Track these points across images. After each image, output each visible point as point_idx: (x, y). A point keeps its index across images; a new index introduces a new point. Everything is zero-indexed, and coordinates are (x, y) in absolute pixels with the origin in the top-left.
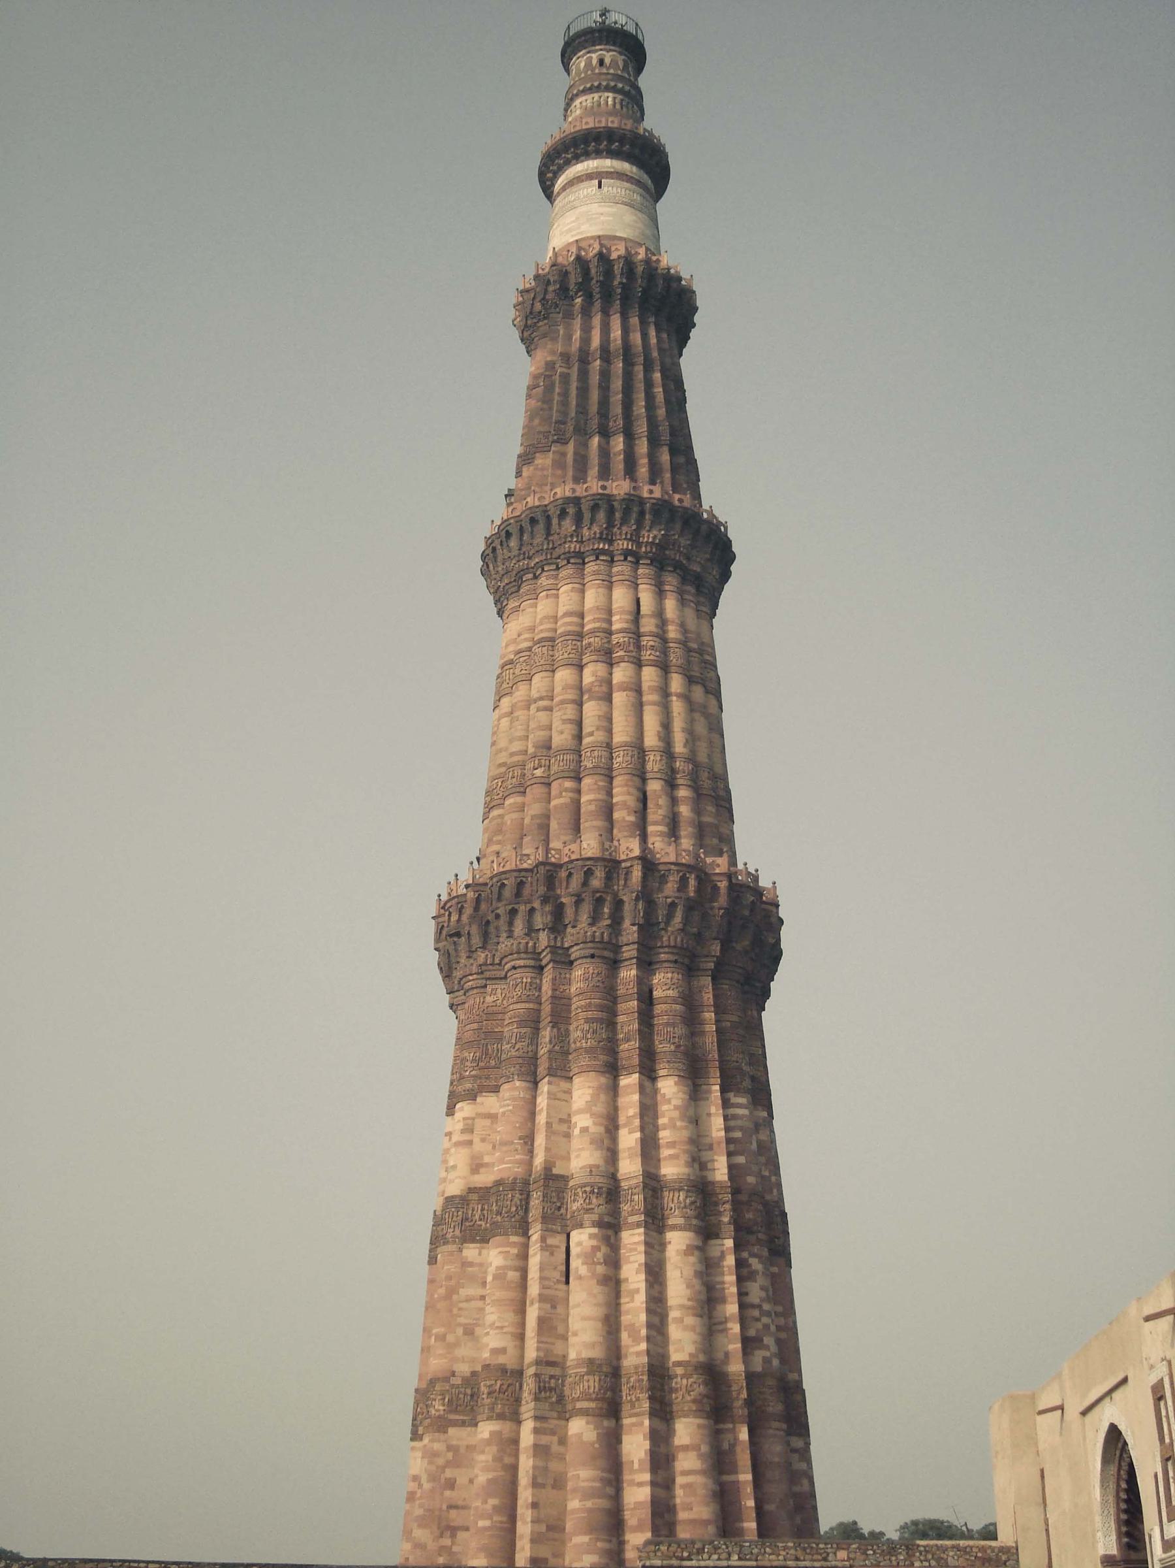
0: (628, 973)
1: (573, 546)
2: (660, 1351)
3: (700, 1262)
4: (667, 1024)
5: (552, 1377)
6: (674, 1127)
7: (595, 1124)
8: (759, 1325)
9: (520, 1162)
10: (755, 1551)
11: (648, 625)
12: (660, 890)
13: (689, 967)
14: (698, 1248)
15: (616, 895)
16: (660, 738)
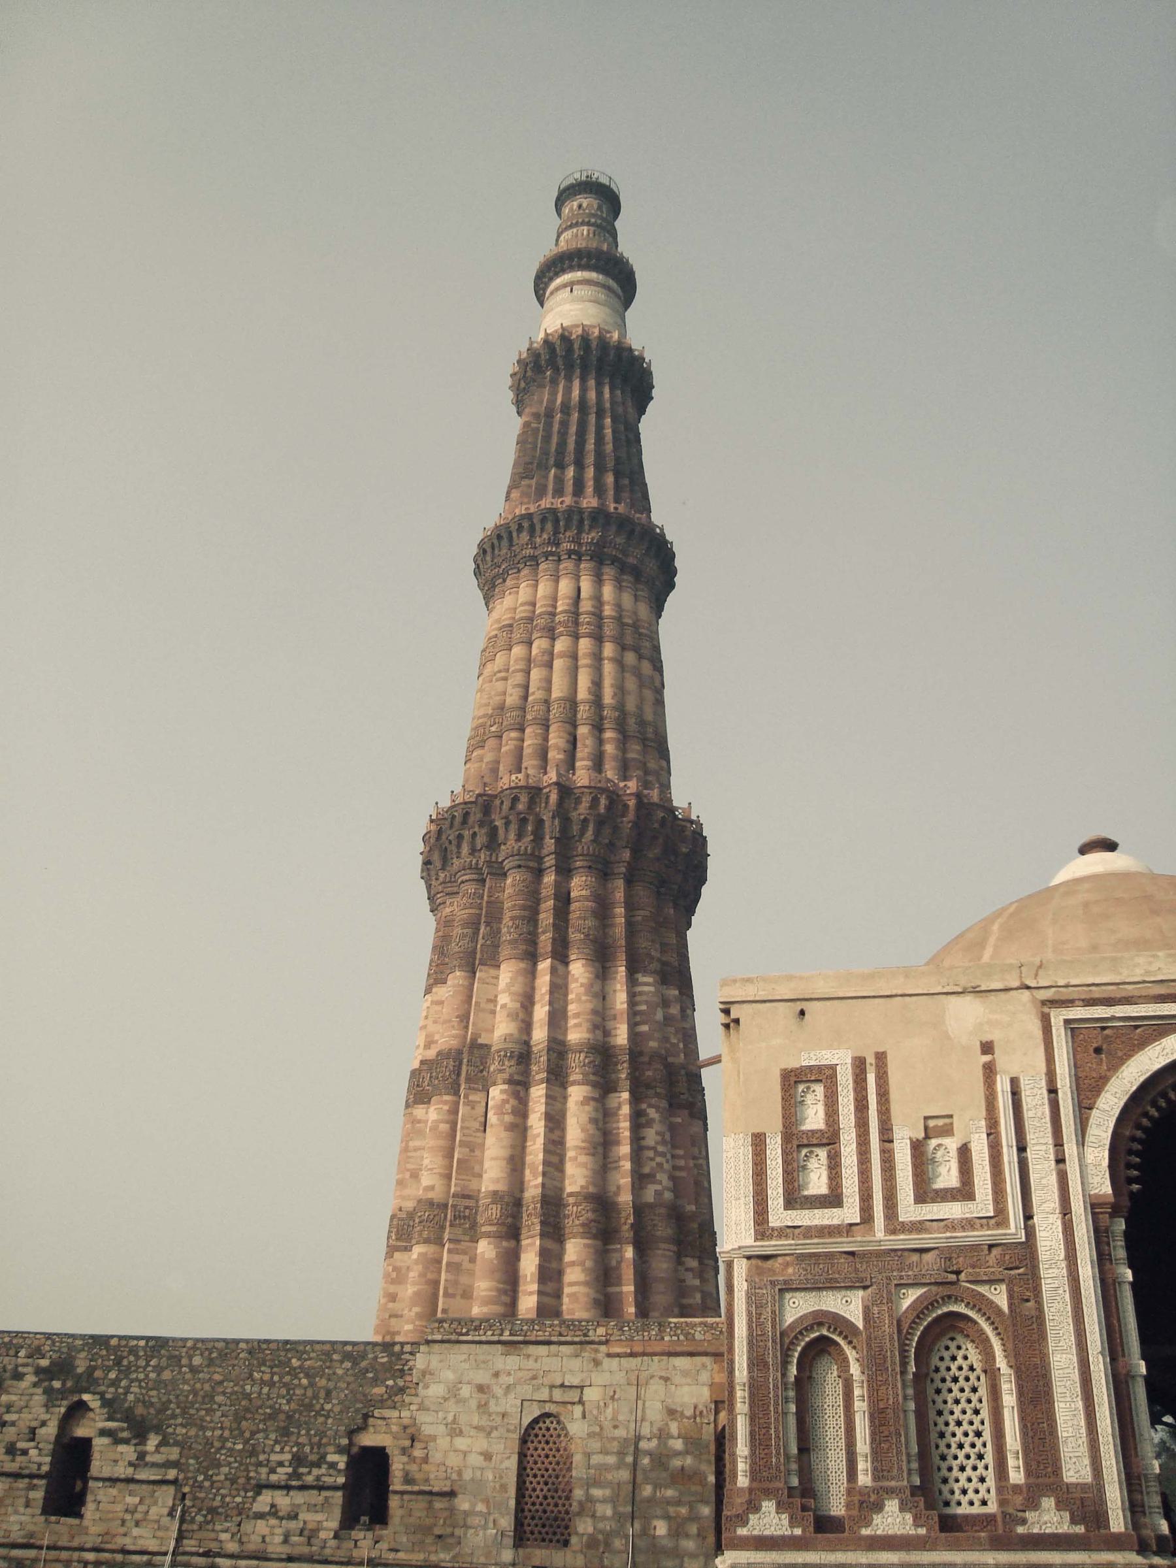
0: (549, 878)
1: (528, 552)
2: (555, 1183)
3: (596, 1110)
4: (579, 918)
5: (466, 1207)
6: (579, 1000)
7: (512, 1001)
8: (653, 1164)
9: (455, 1037)
10: (525, 1328)
11: (586, 606)
12: (575, 809)
13: (603, 871)
14: (593, 1099)
15: (537, 815)
16: (590, 693)
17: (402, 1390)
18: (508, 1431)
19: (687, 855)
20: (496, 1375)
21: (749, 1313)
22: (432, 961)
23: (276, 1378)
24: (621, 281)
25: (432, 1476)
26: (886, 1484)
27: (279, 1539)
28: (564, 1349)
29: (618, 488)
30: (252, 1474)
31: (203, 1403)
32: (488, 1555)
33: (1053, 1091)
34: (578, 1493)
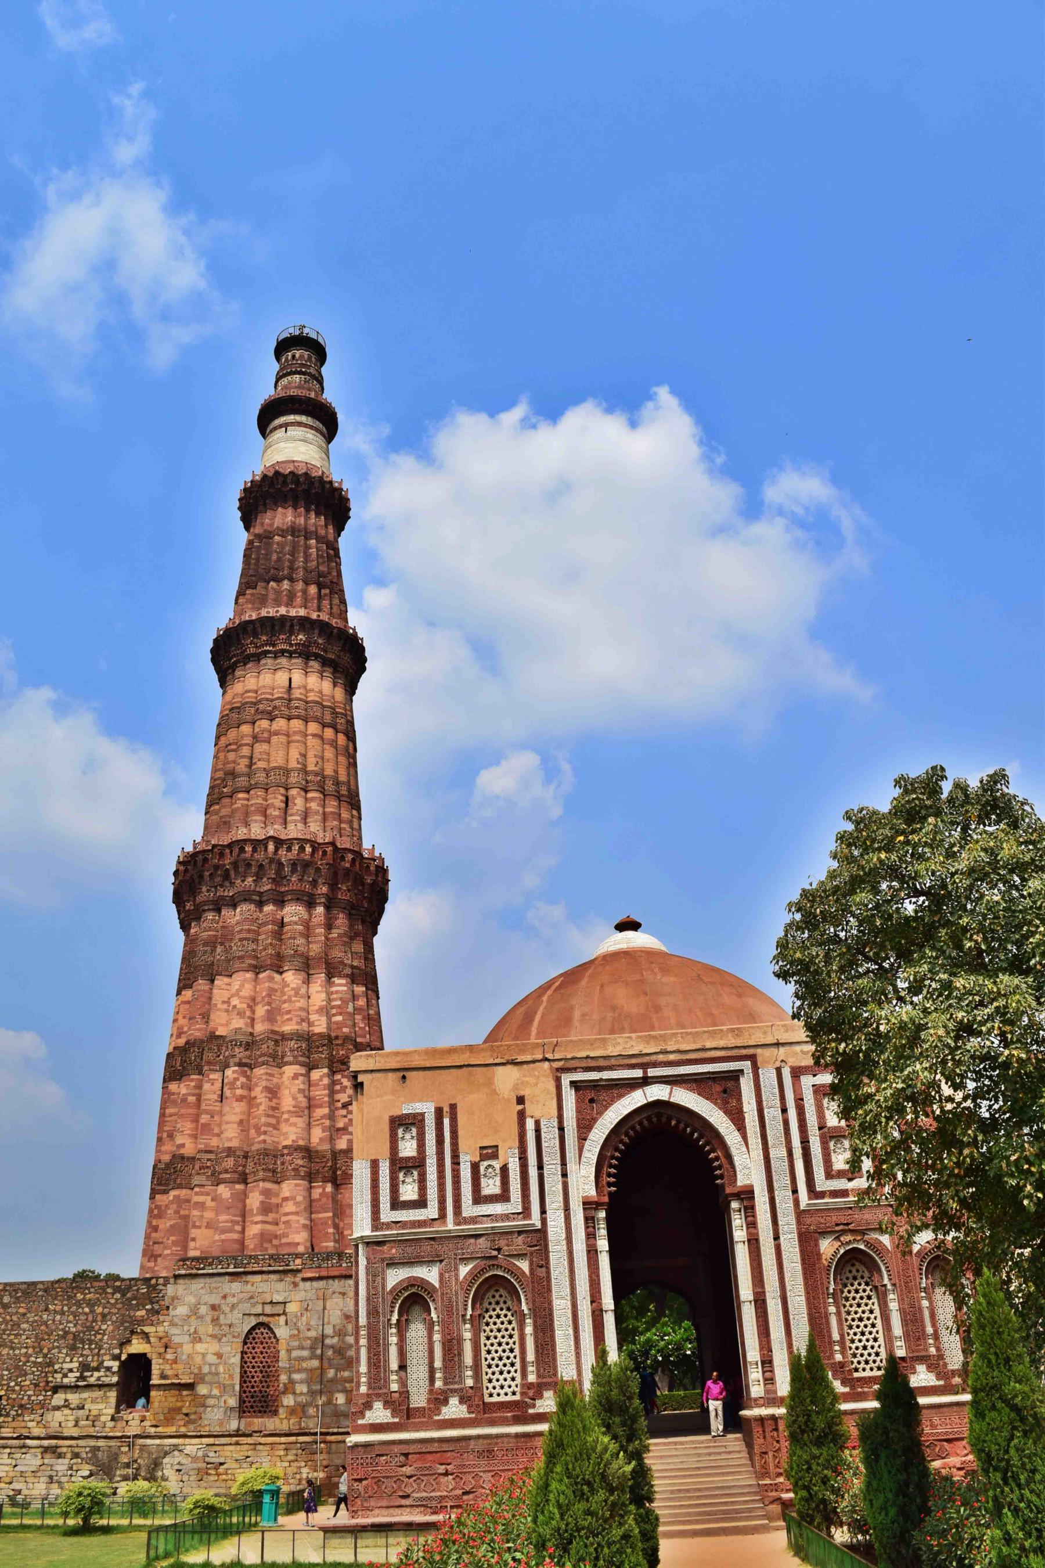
2: (276, 1140)
5: (208, 1160)
7: (241, 1003)
9: (199, 1030)
17: (158, 1313)
18: (234, 1337)
19: (372, 885)
20: (225, 1297)
21: (368, 1280)
22: (181, 969)
23: (66, 1308)
24: (327, 422)
25: (180, 1372)
26: (451, 1387)
27: (71, 1424)
28: (272, 1276)
29: (320, 597)
30: (50, 1379)
31: (12, 1330)
32: (221, 1425)
33: (561, 1129)
34: (283, 1378)
